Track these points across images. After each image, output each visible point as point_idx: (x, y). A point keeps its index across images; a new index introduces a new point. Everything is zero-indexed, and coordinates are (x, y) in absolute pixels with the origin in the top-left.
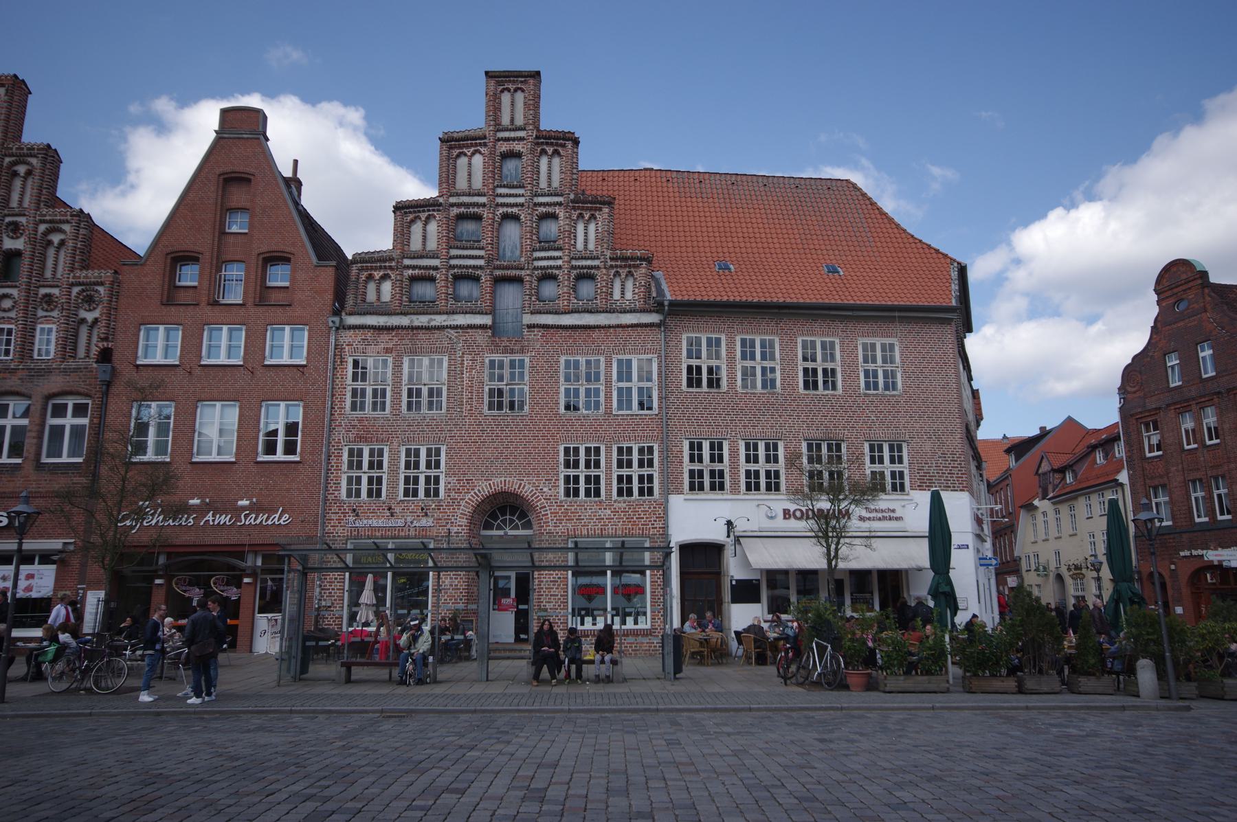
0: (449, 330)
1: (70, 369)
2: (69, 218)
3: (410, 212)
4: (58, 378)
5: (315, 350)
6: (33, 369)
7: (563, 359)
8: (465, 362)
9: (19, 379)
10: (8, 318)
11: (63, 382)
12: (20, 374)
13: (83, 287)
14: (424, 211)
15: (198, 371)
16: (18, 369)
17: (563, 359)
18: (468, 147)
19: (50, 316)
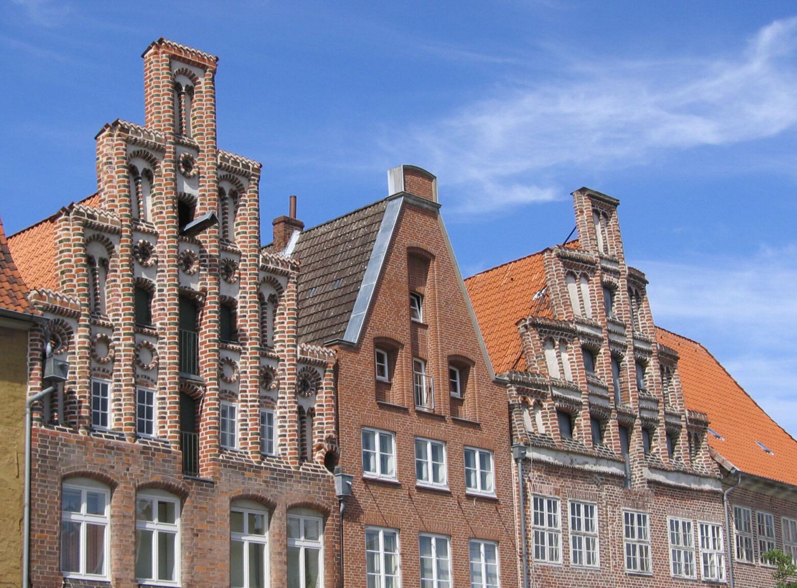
0: (596, 475)
1: (309, 475)
2: (289, 270)
3: (545, 332)
4: (300, 485)
5: (503, 481)
6: (275, 470)
7: (668, 519)
8: (609, 513)
9: (265, 482)
10: (230, 392)
11: (305, 492)
12: (266, 475)
13: (305, 366)
14: (558, 334)
15: (416, 496)
16: (261, 468)
17: (668, 519)
18: (577, 268)
19: (269, 398)
